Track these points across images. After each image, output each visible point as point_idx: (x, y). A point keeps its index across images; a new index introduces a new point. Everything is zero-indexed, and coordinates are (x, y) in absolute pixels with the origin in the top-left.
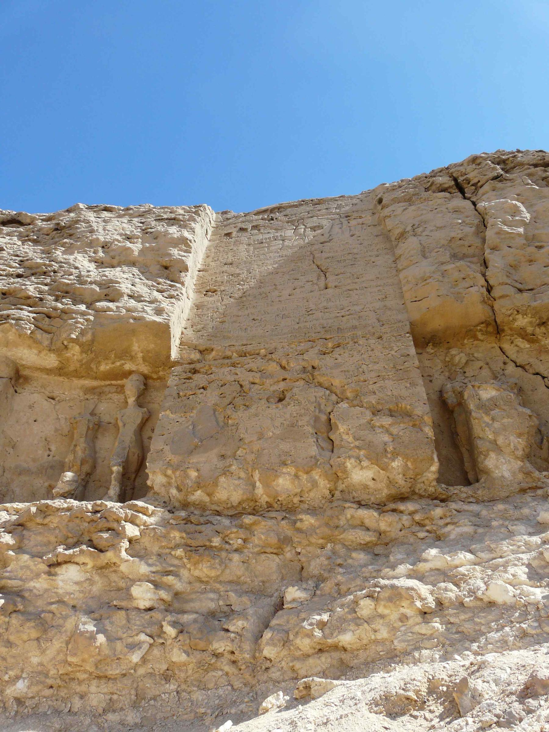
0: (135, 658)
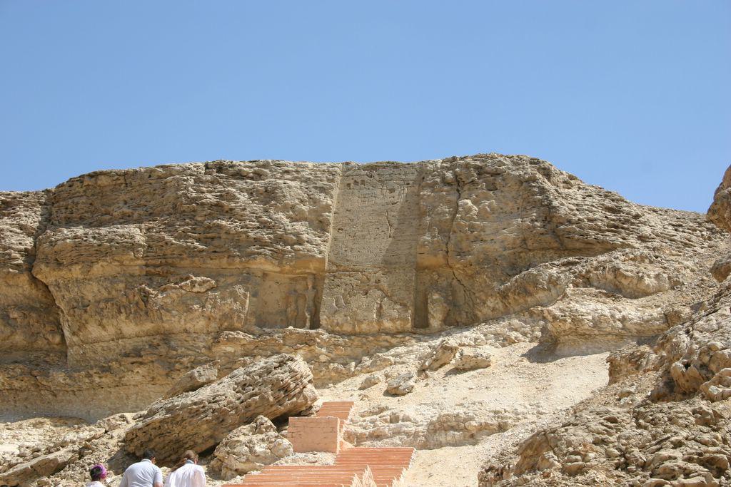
0: (322, 374)
